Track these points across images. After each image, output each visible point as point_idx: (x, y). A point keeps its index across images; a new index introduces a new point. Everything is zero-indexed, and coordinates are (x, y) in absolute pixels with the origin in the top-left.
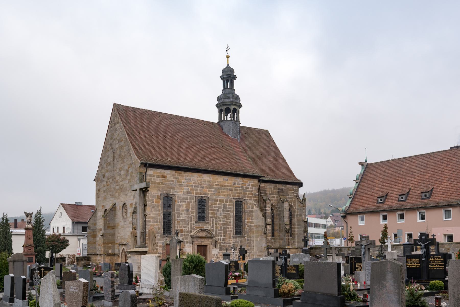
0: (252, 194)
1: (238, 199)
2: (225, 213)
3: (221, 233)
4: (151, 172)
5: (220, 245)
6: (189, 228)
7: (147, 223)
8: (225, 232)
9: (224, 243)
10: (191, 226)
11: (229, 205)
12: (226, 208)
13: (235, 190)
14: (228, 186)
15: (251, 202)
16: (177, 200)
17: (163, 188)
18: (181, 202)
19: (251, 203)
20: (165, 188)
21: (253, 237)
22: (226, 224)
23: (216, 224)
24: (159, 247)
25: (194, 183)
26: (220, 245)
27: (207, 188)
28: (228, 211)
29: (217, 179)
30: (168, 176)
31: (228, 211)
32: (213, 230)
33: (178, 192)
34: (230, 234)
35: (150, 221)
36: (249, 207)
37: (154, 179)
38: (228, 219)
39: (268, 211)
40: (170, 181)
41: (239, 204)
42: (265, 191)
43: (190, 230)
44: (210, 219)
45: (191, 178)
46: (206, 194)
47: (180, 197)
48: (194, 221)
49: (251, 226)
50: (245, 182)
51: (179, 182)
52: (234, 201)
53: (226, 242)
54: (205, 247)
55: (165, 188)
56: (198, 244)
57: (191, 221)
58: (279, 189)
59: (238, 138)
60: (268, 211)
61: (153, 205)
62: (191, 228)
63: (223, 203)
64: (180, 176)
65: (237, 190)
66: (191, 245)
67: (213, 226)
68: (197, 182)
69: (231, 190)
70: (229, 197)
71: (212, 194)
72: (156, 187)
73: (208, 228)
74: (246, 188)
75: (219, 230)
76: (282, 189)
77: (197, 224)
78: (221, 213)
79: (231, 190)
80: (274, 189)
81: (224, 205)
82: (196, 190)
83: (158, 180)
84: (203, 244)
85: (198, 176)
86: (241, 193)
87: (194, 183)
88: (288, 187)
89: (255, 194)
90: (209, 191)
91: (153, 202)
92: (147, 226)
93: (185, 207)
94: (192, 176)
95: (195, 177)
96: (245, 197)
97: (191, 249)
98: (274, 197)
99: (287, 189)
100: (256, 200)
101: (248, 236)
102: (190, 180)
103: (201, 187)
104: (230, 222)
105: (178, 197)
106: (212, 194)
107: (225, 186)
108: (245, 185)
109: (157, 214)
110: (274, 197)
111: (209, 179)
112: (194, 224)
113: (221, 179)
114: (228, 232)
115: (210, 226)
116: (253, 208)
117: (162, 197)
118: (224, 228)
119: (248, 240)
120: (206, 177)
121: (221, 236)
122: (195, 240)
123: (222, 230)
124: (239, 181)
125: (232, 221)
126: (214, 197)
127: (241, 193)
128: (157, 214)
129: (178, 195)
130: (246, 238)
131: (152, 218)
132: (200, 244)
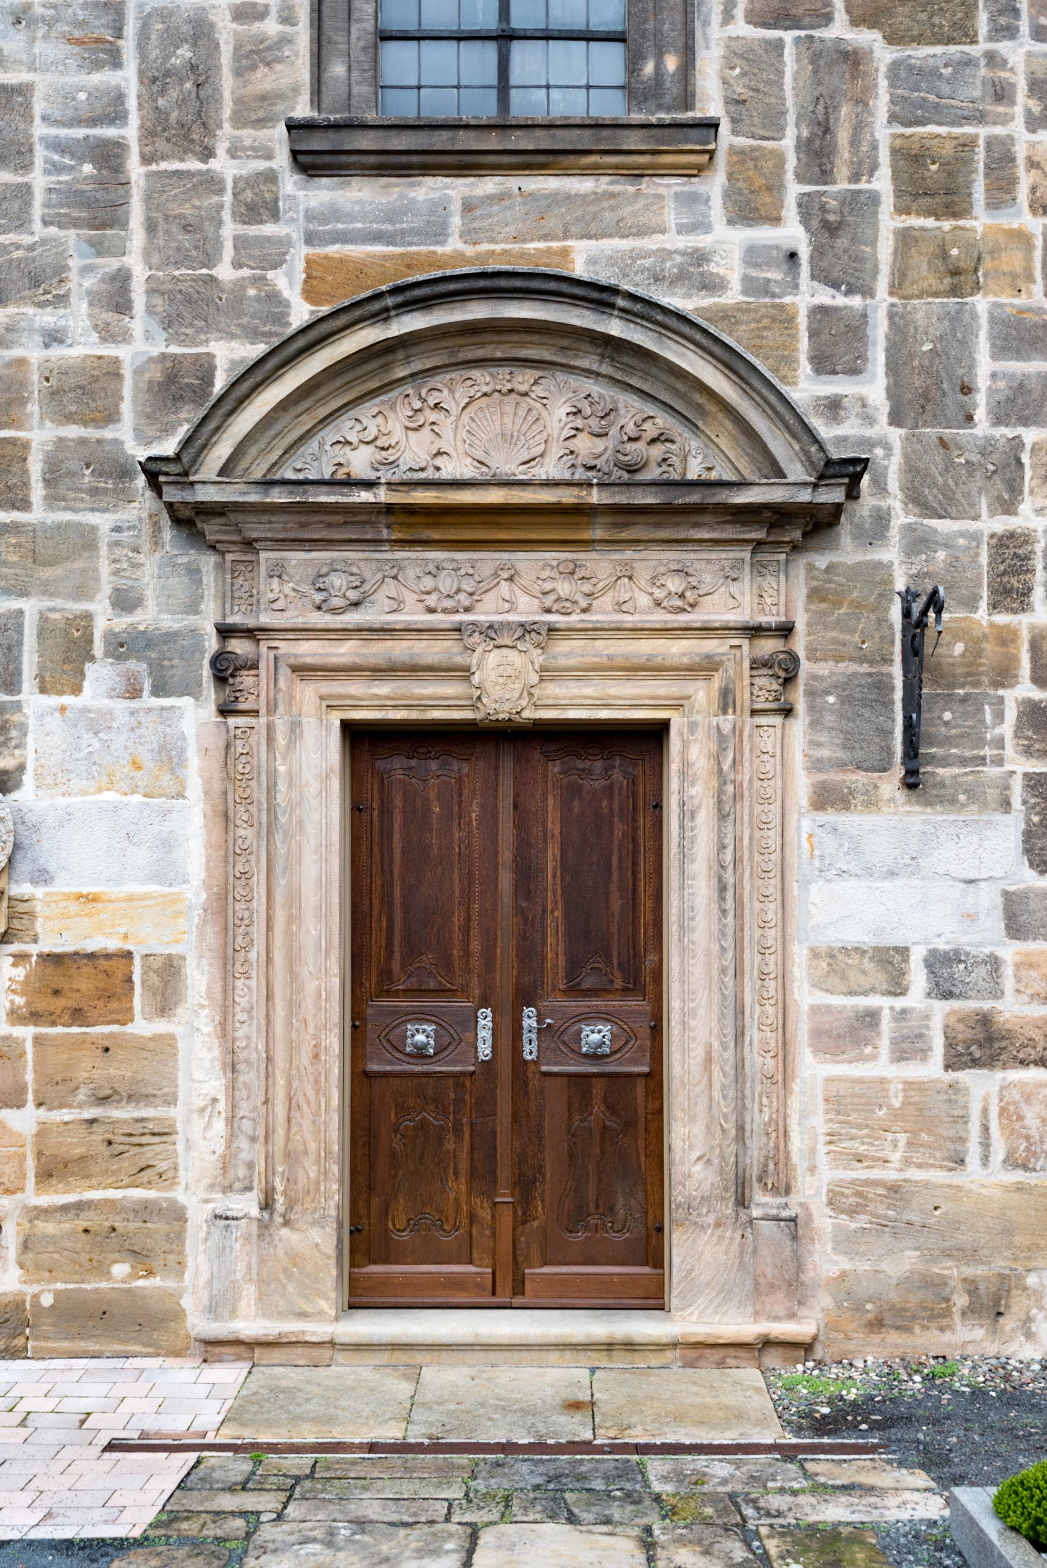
6: (116, 296)
10: (185, 236)
32: (837, 345)
43: (143, 345)
44: (755, 63)
48: (253, 111)
54: (597, 773)
56: (381, 702)
57: (184, 128)
62: (189, 306)
66: (195, 715)
73: (696, 271)
75: (1018, 336)
77: (360, 195)
84: (506, 686)
97: (192, 823)
112: (258, 204)
115: (728, 244)
122: (288, 588)
132: (438, 701)
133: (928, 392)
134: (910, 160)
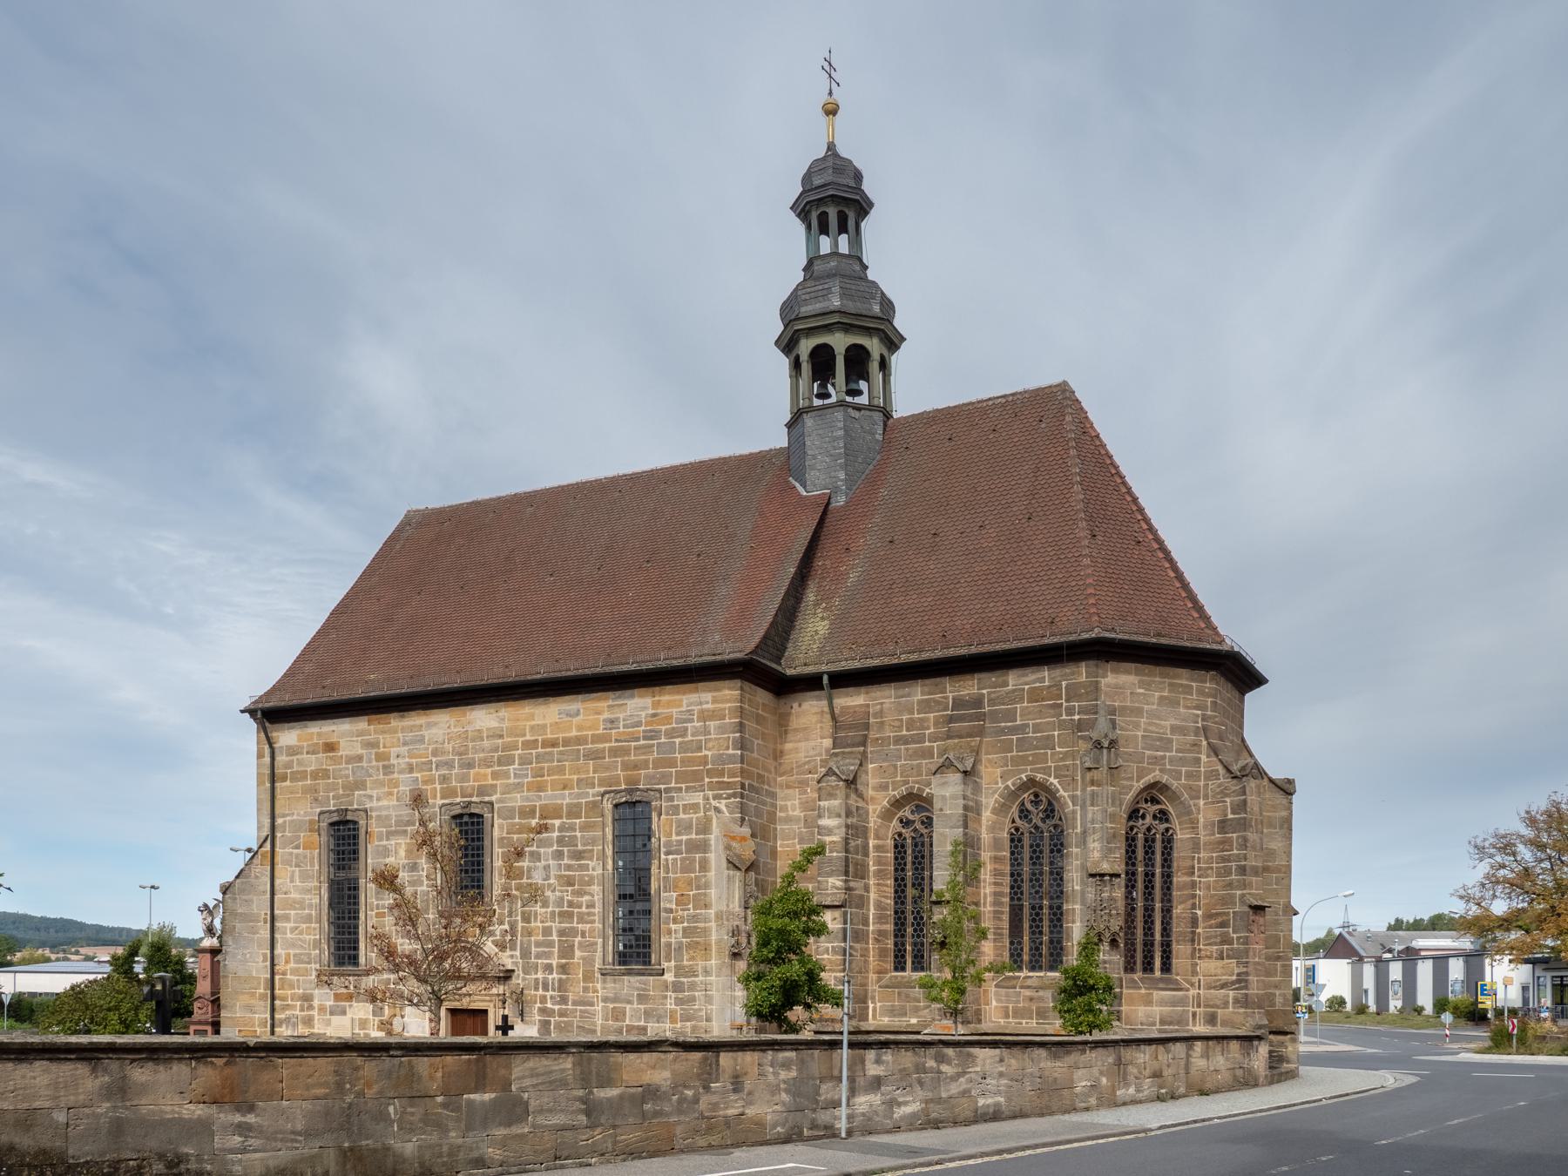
0: (704, 760)
1: (630, 791)
2: (569, 867)
3: (548, 955)
4: (288, 736)
5: (543, 1011)
7: (277, 924)
8: (567, 951)
9: (564, 1000)
11: (583, 828)
12: (572, 842)
13: (614, 752)
14: (580, 740)
15: (697, 798)
16: (375, 828)
17: (328, 788)
18: (389, 835)
19: (695, 807)
20: (334, 787)
21: (707, 972)
22: (570, 915)
23: (526, 919)
24: (315, 1013)
25: (435, 754)
26: (543, 1011)
27: (486, 763)
28: (578, 855)
29: (532, 717)
30: (342, 744)
31: (578, 855)
33: (378, 799)
34: (588, 961)
35: (287, 918)
36: (685, 827)
37: (300, 763)
38: (580, 893)
39: (830, 832)
40: (350, 760)
41: (633, 818)
42: (867, 726)
45: (426, 733)
46: (482, 791)
47: (388, 817)
49: (695, 918)
50: (669, 704)
51: (379, 757)
52: (608, 806)
53: (571, 996)
55: (334, 787)
58: (959, 703)
59: (836, 490)
60: (830, 832)
61: (297, 856)
63: (557, 822)
64: (383, 732)
65: (626, 751)
67: (513, 926)
68: (449, 747)
69: (595, 756)
70: (583, 791)
71: (508, 789)
72: (306, 790)
74: (671, 734)
75: (538, 944)
76: (978, 702)
78: (547, 868)
79: (595, 756)
80: (926, 706)
81: (561, 829)
82: (444, 779)
83: (312, 762)
85: (452, 721)
86: (645, 764)
87: (435, 754)
88: (1015, 680)
89: (720, 759)
90: (495, 775)
91: (297, 847)
92: (277, 936)
93: (402, 853)
94: (429, 725)
95: (440, 725)
96: (665, 778)
98: (928, 754)
99: (1016, 697)
100: (728, 785)
101: (679, 971)
102: (422, 740)
103: (461, 766)
104: (591, 905)
105: (379, 817)
106: (508, 789)
107: (567, 742)
108: (668, 719)
109: (309, 891)
110: (928, 754)
111: (494, 724)
113: (548, 715)
114: (578, 953)
116: (705, 828)
117: (324, 825)
118: (562, 933)
119: (677, 987)
120: (483, 718)
121: (548, 968)
123: (551, 944)
124: (638, 705)
125: (597, 898)
126: (517, 800)
127: (645, 764)
128: (309, 891)
129: (379, 809)
130: (669, 977)
131: (292, 904)
133: (525, 954)
134: (523, 913)
